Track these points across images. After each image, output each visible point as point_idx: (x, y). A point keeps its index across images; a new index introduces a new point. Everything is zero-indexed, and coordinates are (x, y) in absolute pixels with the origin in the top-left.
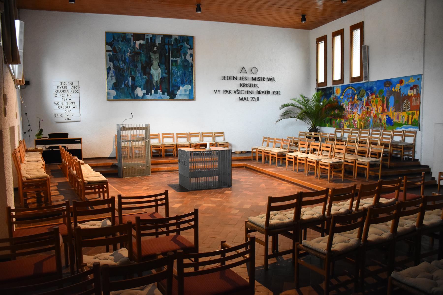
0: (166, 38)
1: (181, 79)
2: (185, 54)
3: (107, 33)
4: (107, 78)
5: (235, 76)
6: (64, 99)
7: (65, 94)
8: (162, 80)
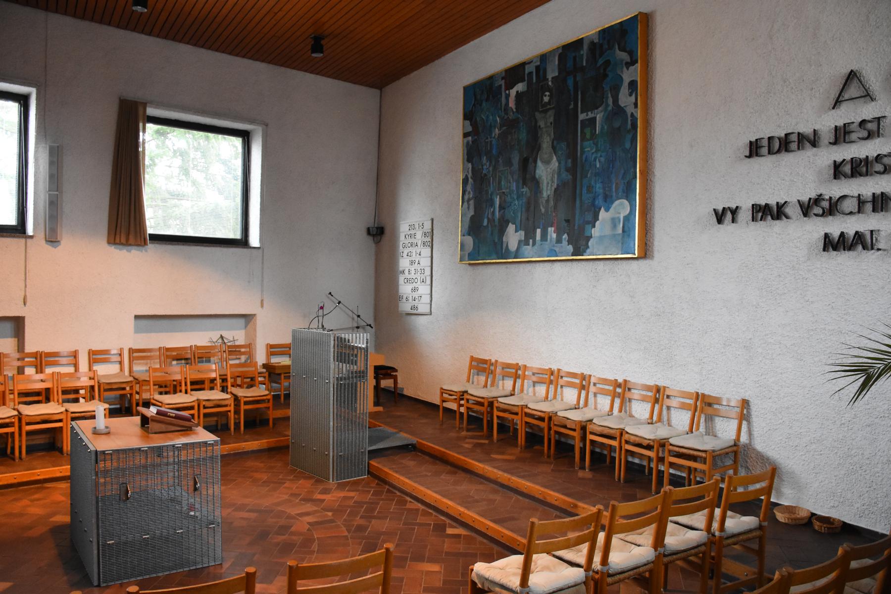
2: (616, 89)
5: (807, 130)
6: (412, 263)
7: (413, 250)
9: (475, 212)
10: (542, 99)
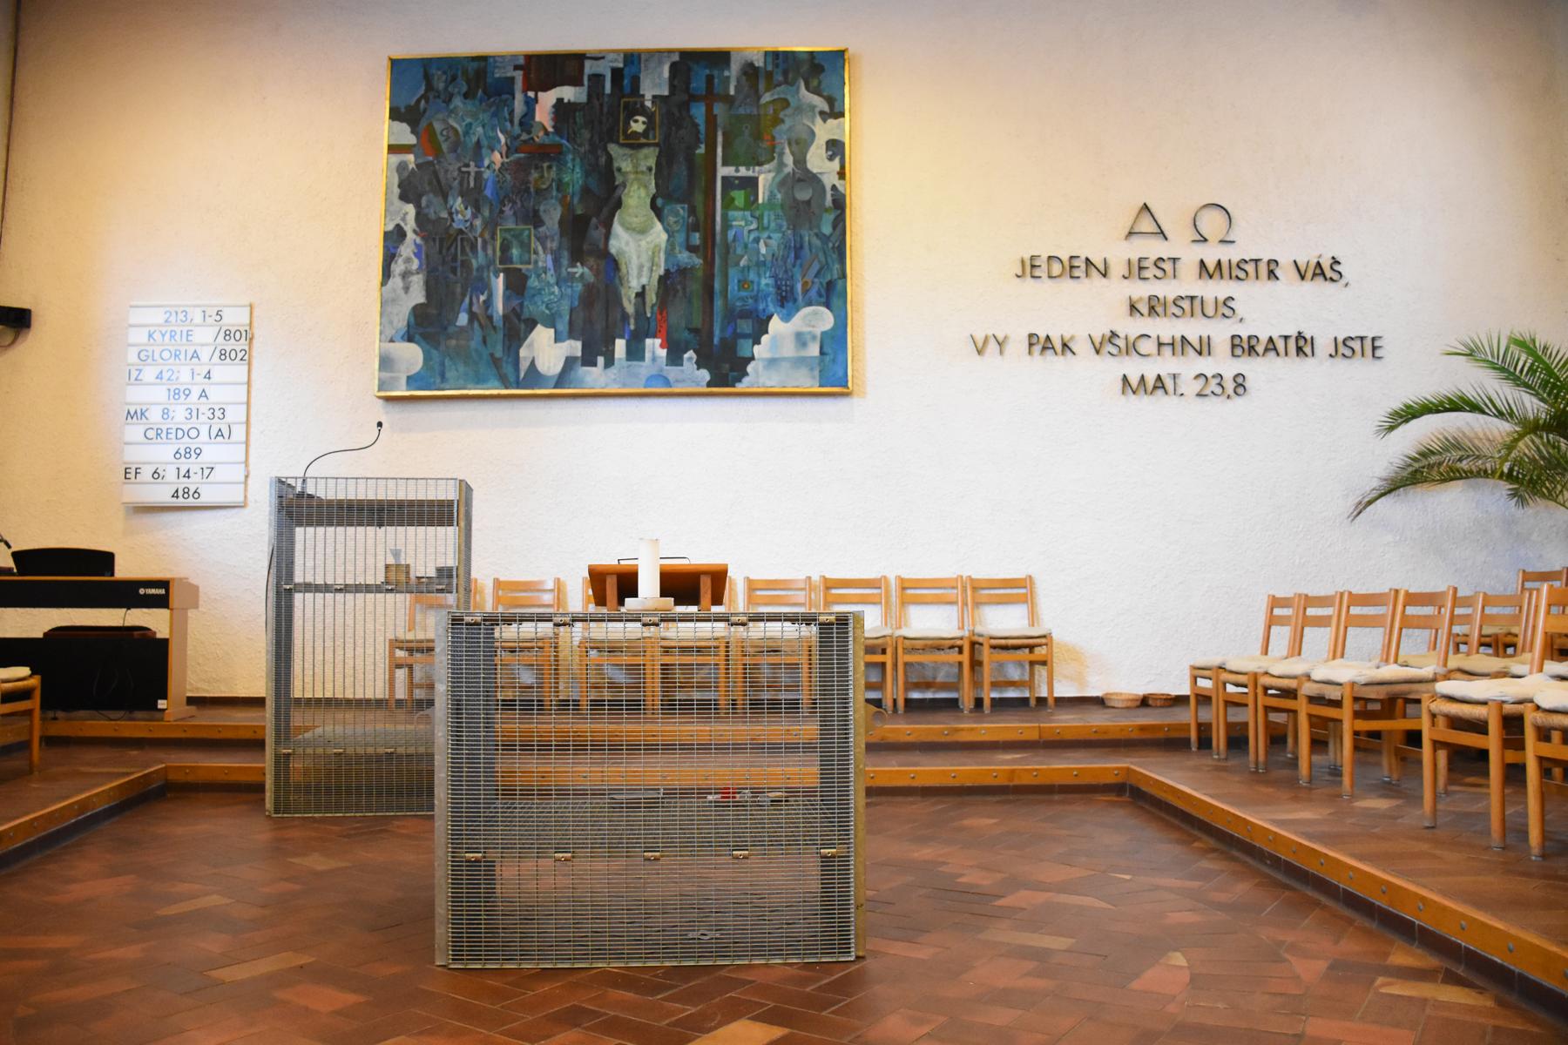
0: (697, 68)
1: (775, 277)
2: (801, 146)
3: (397, 65)
4: (384, 283)
9: (428, 296)
10: (627, 125)
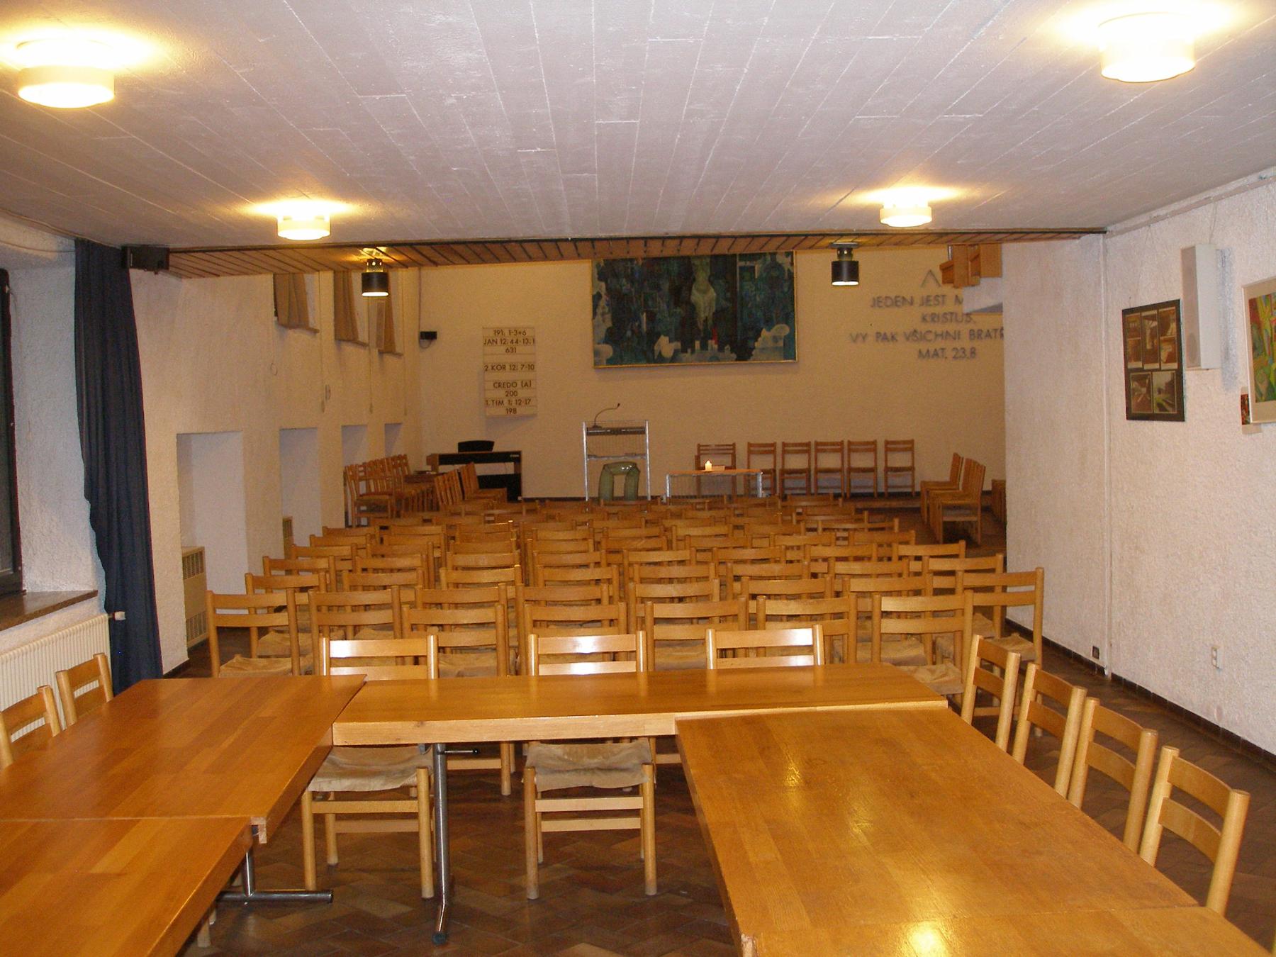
5: (908, 298)
8: (719, 314)
